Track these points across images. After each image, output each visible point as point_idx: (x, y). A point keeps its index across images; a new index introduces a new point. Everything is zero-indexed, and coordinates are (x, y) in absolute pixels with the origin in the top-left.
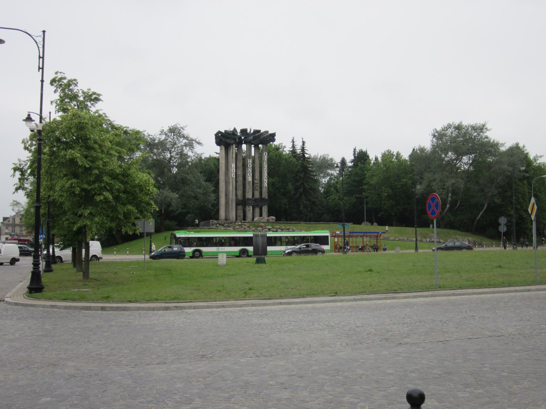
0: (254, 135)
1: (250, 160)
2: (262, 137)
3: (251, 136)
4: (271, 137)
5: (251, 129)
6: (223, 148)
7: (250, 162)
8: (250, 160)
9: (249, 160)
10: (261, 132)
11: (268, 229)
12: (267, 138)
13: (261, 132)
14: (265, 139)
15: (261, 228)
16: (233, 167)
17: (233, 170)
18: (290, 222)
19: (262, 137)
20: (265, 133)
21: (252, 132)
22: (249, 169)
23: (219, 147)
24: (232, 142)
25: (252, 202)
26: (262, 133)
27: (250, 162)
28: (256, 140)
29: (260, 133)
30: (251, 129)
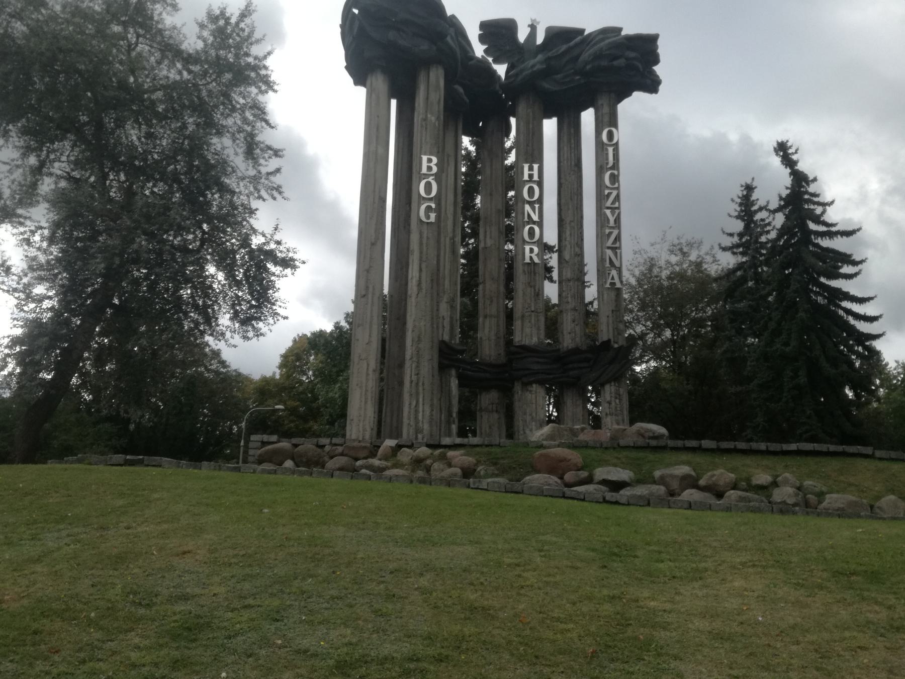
0: (550, 54)
1: (531, 169)
2: (585, 56)
3: (535, 57)
4: (632, 55)
5: (533, 27)
6: (380, 82)
7: (531, 176)
8: (531, 169)
9: (526, 167)
10: (586, 33)
11: (604, 482)
12: (616, 58)
13: (586, 33)
14: (604, 63)
15: (554, 479)
16: (424, 170)
17: (428, 187)
18: (774, 447)
19: (591, 51)
20: (601, 36)
21: (540, 39)
22: (527, 208)
23: (362, 91)
24: (425, 46)
25: (536, 367)
26: (590, 34)
27: (531, 176)
28: (559, 76)
29: (579, 38)
30: (533, 27)
